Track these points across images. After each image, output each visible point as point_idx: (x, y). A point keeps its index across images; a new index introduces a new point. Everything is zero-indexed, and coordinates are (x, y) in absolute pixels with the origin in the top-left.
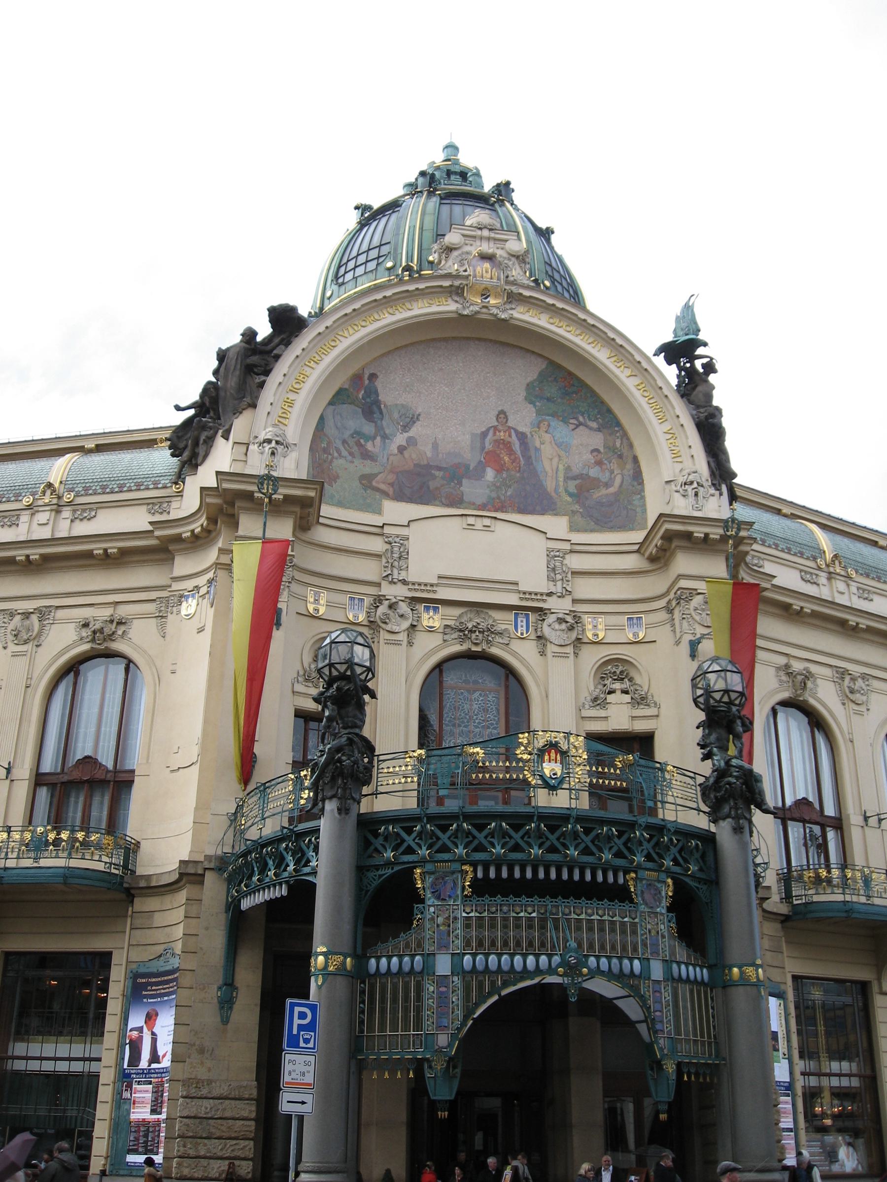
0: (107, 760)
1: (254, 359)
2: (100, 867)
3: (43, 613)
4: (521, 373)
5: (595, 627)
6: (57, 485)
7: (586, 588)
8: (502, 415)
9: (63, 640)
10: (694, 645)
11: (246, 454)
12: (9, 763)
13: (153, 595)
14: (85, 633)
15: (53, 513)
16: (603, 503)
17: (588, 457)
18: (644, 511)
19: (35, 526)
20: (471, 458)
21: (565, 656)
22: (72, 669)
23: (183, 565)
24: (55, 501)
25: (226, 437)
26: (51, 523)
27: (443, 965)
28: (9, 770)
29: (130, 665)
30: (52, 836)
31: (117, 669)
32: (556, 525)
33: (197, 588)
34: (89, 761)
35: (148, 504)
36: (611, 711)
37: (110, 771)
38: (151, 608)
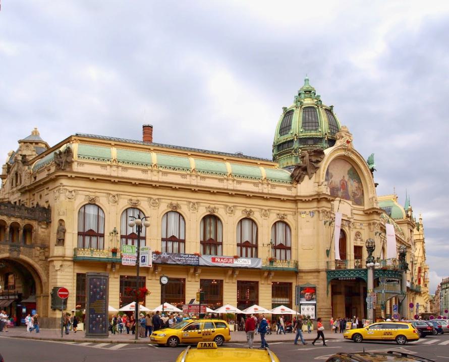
0: (284, 245)
1: (310, 158)
4: (348, 167)
5: (358, 225)
7: (356, 217)
8: (344, 177)
10: (376, 234)
11: (319, 186)
13: (292, 210)
14: (278, 216)
16: (359, 201)
17: (355, 188)
18: (364, 202)
20: (339, 186)
21: (352, 231)
23: (300, 205)
25: (310, 179)
27: (383, 292)
29: (287, 224)
32: (350, 202)
33: (305, 212)
34: (281, 244)
36: (358, 242)
38: (291, 213)
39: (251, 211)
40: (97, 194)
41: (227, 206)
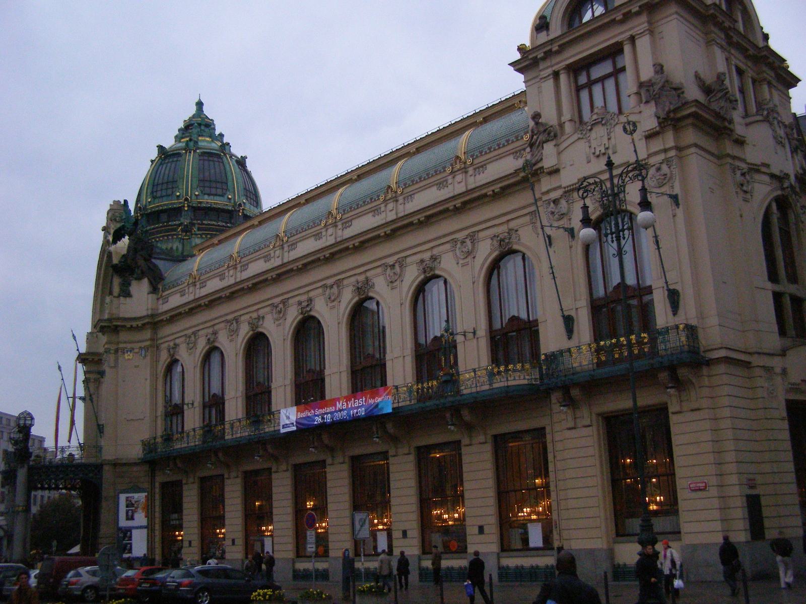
0: (524, 316)
2: (526, 382)
3: (473, 237)
6: (463, 157)
9: (485, 251)
12: (474, 329)
15: (464, 174)
19: (456, 184)
22: (495, 267)
24: (463, 166)
26: (464, 180)
28: (474, 333)
30: (496, 370)
31: (519, 258)
35: (513, 153)
37: (525, 322)
38: (528, 218)
39: (434, 258)
40: (216, 327)
41: (385, 266)
